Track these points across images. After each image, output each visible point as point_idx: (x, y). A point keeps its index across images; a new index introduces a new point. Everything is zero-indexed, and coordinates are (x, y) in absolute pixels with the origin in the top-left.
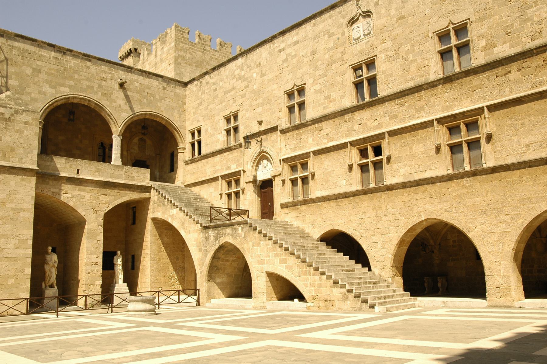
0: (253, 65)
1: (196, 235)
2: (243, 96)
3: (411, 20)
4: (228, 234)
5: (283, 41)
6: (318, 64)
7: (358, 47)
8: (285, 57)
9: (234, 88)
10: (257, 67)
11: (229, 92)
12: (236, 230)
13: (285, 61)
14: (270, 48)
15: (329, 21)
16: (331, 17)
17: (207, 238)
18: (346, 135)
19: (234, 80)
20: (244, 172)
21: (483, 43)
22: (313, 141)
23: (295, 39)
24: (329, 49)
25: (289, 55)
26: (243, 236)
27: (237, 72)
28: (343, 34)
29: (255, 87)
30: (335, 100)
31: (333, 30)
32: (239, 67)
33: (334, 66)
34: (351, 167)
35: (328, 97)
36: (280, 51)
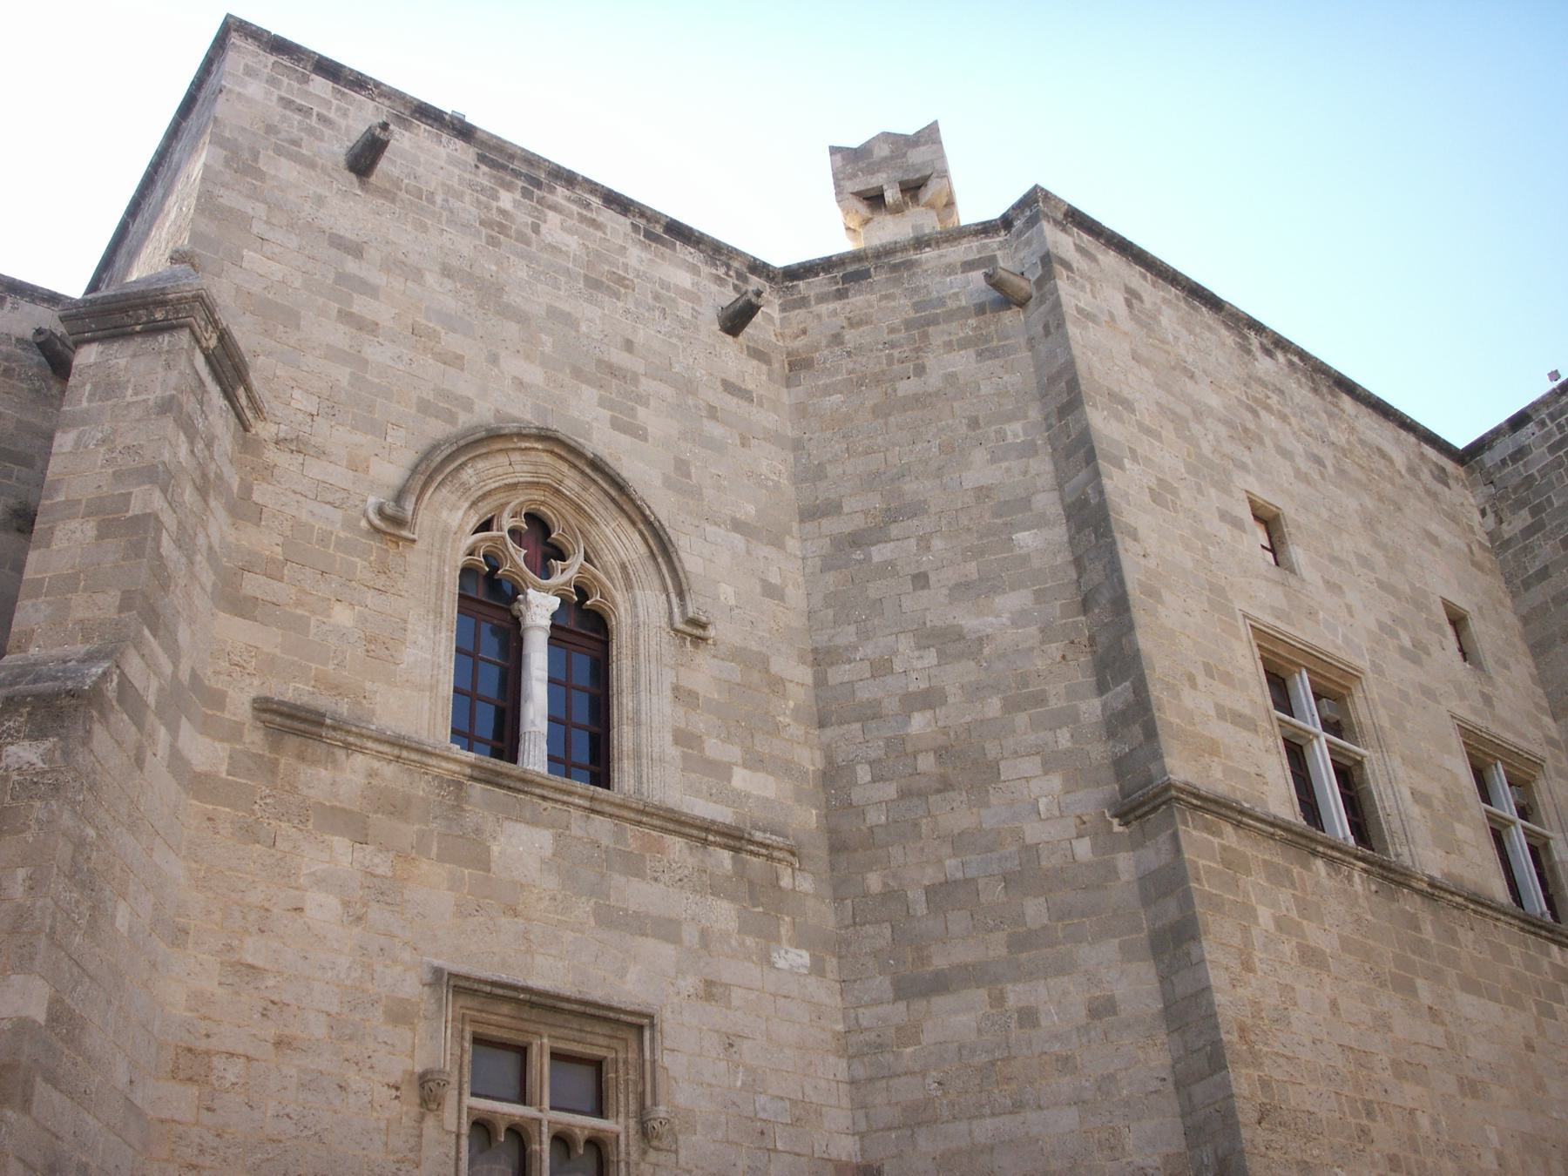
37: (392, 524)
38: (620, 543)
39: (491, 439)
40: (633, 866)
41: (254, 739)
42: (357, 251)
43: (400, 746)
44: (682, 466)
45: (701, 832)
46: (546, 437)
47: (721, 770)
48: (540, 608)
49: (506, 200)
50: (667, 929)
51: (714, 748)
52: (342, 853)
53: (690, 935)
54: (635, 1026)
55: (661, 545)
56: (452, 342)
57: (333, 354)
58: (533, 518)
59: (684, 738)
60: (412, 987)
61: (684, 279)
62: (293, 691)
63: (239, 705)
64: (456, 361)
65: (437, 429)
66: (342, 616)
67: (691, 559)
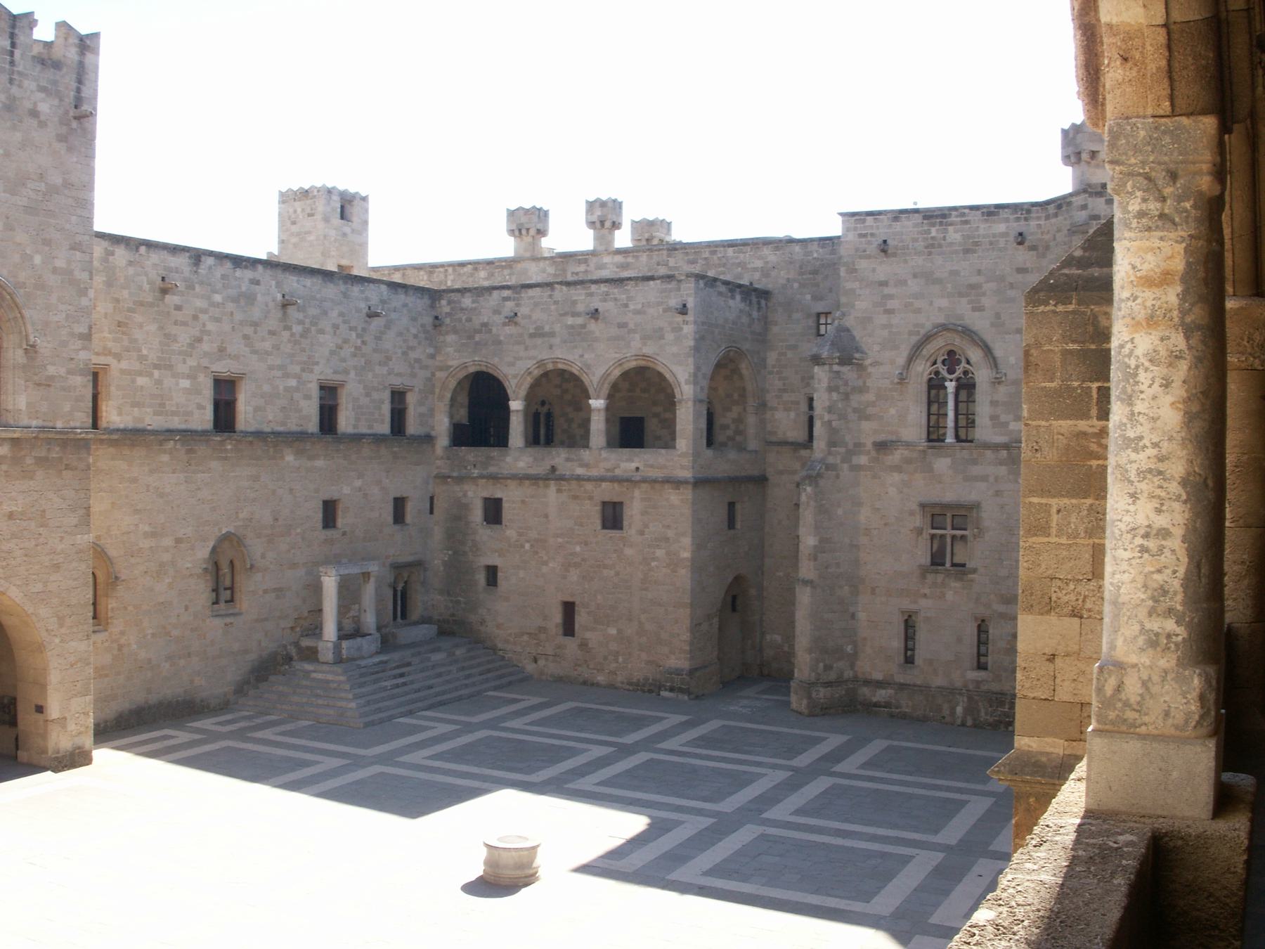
37: (902, 380)
38: (975, 355)
39: (928, 338)
40: (974, 462)
41: (873, 453)
42: (884, 284)
43: (908, 445)
44: (998, 316)
45: (996, 447)
46: (944, 328)
47: (1006, 424)
48: (951, 386)
49: (934, 232)
50: (984, 478)
51: (1003, 418)
52: (896, 477)
53: (991, 479)
54: (975, 507)
55: (987, 350)
56: (918, 304)
57: (884, 327)
58: (951, 353)
59: (994, 418)
60: (915, 507)
61: (1001, 228)
62: (881, 437)
63: (869, 446)
64: (919, 311)
65: (914, 339)
66: (893, 411)
67: (998, 353)
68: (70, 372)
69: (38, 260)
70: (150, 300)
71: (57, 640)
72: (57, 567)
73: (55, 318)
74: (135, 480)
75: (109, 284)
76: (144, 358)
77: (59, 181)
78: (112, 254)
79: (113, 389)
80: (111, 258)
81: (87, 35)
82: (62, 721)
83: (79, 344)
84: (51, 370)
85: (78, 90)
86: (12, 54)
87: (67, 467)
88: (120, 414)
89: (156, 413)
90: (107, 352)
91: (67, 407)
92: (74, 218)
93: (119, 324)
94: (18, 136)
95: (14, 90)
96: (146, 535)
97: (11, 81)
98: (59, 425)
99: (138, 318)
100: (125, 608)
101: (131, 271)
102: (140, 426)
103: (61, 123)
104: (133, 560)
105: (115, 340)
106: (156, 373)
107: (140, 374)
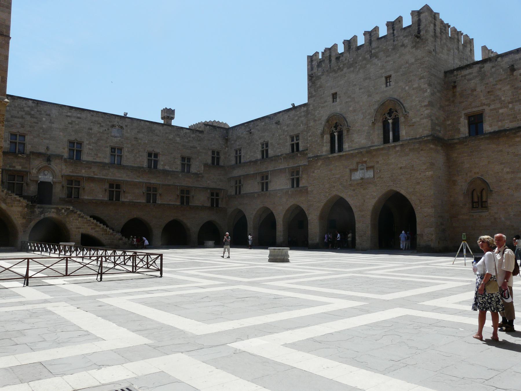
0: (43, 112)
1: (20, 209)
2: (30, 127)
3: (140, 141)
4: (53, 212)
5: (70, 112)
6: (93, 136)
7: (115, 140)
8: (70, 121)
9: (24, 118)
10: (47, 115)
11: (16, 117)
12: (60, 210)
13: (69, 123)
14: (59, 110)
15: (101, 119)
16: (102, 117)
17: (33, 212)
18: (105, 175)
19: (23, 113)
20: (30, 173)
21: (162, 163)
22: (85, 172)
23: (79, 115)
24: (99, 132)
25: (74, 122)
26: (66, 214)
27: (27, 109)
28: (108, 129)
29: (44, 126)
30: (100, 157)
31: (102, 124)
32: (29, 107)
33: (101, 141)
34: (106, 190)
35: (97, 155)
36: (67, 116)
68: (421, 119)
69: (407, 88)
70: (505, 77)
71: (419, 208)
72: (418, 183)
73: (415, 104)
74: (501, 151)
75: (482, 80)
76: (504, 101)
77: (413, 60)
78: (483, 67)
79: (487, 118)
80: (482, 69)
81: (421, 9)
82: (422, 235)
83: (424, 109)
84: (414, 120)
85: (419, 28)
86: (393, 33)
87: (422, 150)
88: (491, 126)
89: (511, 122)
90: (484, 104)
91: (421, 130)
92: (420, 70)
93: (489, 92)
94: (398, 55)
95: (396, 43)
96: (508, 173)
97: (394, 41)
98: (418, 136)
99: (499, 86)
100: (498, 203)
101: (493, 70)
102: (502, 129)
103: (413, 43)
104: (501, 184)
105: (486, 99)
106: (510, 106)
107: (501, 108)
